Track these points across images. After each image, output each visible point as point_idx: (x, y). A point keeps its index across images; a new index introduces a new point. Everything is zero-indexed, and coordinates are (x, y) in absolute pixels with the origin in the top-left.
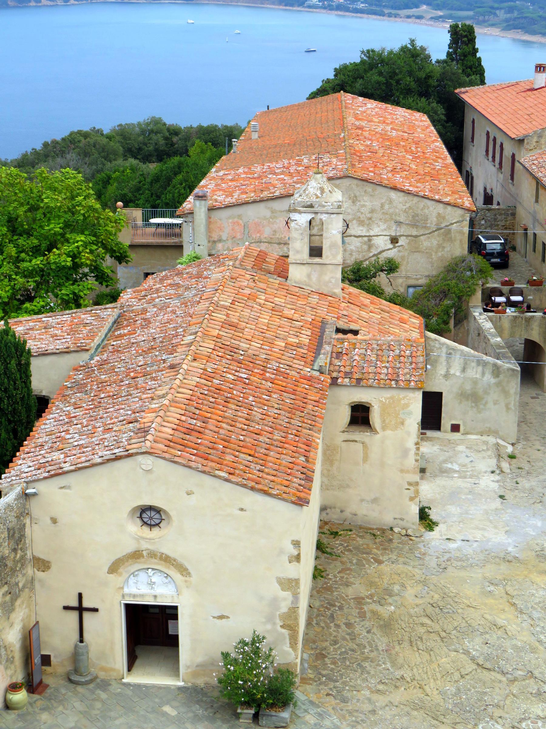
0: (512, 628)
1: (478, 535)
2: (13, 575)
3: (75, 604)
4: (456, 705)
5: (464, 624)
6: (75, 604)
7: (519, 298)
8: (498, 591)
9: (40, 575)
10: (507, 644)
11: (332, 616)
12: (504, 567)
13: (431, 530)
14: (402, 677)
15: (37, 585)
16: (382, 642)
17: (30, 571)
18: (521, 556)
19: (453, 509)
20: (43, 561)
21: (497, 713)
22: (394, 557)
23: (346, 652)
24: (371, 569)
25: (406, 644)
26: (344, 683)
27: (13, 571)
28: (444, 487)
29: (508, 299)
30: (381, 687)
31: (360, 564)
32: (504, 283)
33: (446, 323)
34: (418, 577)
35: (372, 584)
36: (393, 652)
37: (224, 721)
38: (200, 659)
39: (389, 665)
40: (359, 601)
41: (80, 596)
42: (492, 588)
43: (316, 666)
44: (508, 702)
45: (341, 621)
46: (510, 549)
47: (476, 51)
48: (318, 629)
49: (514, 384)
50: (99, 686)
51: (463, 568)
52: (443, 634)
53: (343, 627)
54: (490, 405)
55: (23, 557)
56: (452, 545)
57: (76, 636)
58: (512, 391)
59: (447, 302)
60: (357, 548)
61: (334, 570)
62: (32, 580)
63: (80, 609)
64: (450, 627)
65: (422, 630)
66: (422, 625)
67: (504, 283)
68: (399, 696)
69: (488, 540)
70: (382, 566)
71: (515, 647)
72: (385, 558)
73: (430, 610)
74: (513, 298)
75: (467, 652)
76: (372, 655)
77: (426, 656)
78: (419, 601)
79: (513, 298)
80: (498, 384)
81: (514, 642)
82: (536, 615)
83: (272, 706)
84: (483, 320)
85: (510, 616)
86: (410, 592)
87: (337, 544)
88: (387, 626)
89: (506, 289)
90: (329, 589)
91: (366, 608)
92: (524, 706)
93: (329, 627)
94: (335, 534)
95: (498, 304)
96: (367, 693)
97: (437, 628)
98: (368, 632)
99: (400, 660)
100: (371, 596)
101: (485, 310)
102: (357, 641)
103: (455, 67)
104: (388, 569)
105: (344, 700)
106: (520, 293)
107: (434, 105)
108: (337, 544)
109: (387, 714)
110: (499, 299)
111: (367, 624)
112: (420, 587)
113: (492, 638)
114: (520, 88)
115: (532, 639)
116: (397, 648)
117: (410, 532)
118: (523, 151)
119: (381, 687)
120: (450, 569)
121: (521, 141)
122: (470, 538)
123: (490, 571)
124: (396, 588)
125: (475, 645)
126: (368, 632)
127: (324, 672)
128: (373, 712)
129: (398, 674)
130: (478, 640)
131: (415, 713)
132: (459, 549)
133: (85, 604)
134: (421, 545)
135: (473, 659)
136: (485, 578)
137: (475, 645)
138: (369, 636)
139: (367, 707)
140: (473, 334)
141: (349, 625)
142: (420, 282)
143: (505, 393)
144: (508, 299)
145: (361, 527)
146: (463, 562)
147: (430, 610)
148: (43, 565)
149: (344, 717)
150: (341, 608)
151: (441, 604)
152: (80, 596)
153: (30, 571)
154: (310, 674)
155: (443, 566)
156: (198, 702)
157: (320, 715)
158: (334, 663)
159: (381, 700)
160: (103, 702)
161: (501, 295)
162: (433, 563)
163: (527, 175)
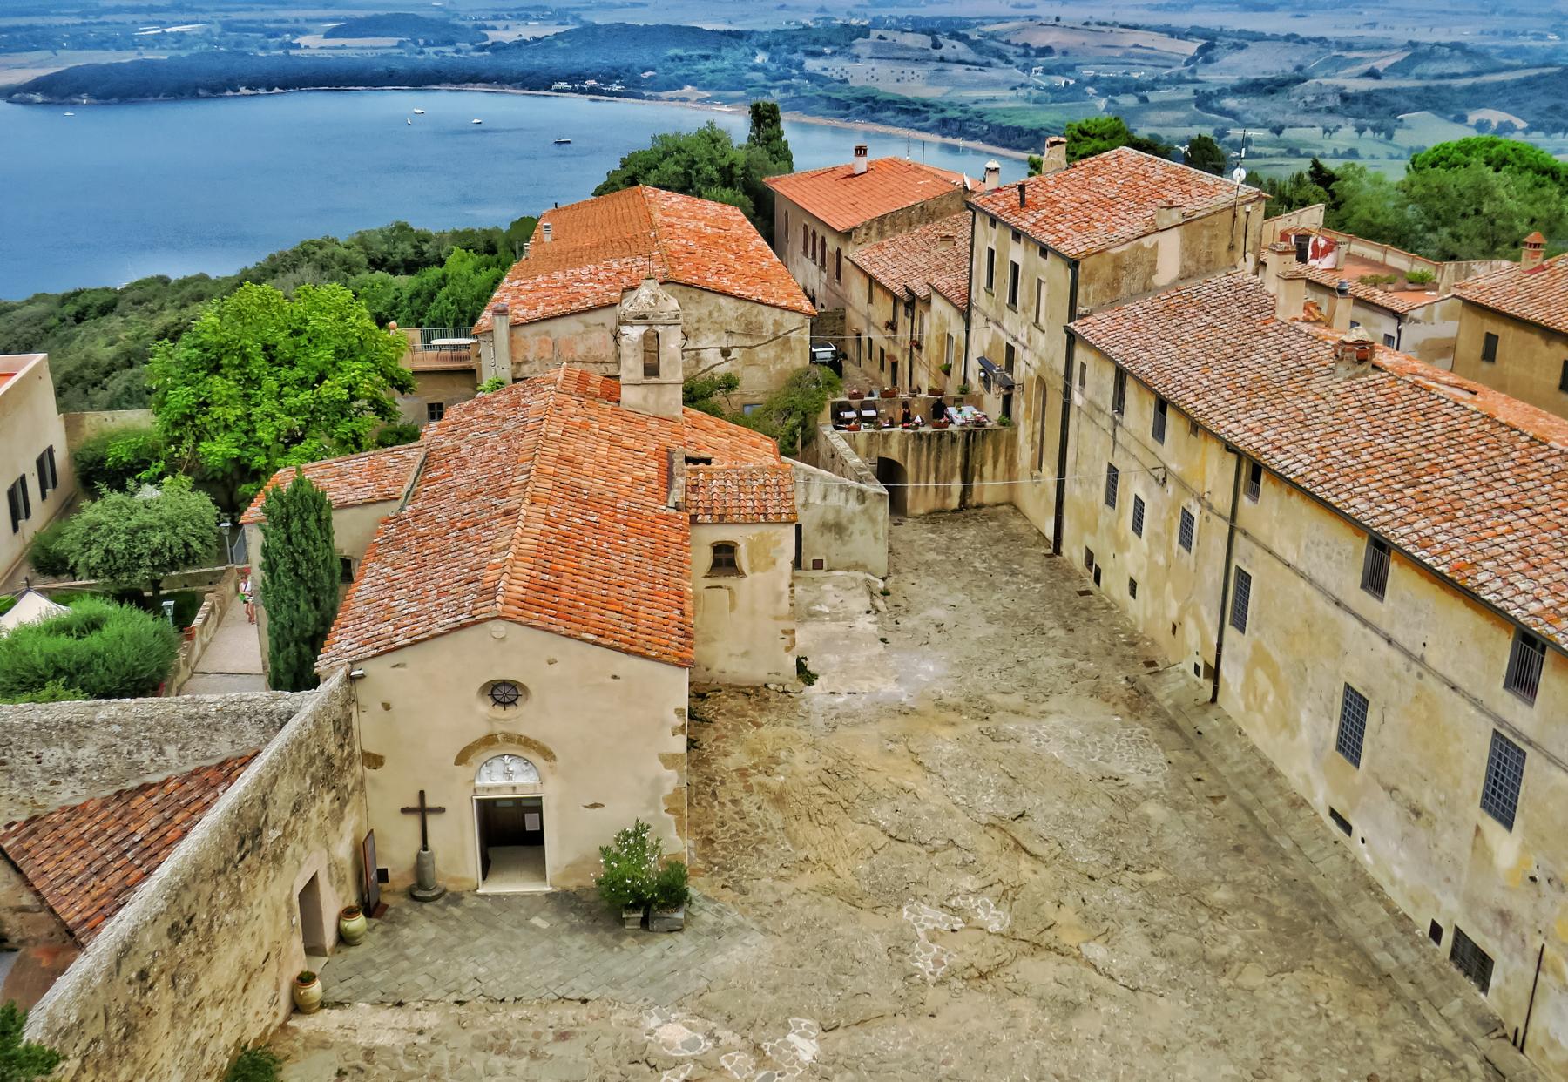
0: (923, 791)
1: (866, 686)
2: (340, 777)
3: (415, 803)
4: (873, 886)
5: (867, 791)
6: (415, 803)
7: (872, 413)
8: (899, 748)
9: (371, 773)
10: (919, 809)
11: (714, 793)
12: (901, 720)
13: (811, 683)
14: (807, 859)
15: (368, 786)
16: (776, 818)
17: (358, 769)
18: (918, 706)
19: (832, 658)
20: (375, 756)
21: (921, 891)
22: (773, 717)
23: (736, 835)
24: (750, 734)
25: (805, 819)
26: (740, 871)
27: (341, 771)
28: (817, 633)
29: (859, 414)
30: (783, 872)
31: (735, 729)
32: (853, 396)
33: (792, 444)
34: (805, 740)
35: (753, 752)
36: (791, 830)
37: (607, 929)
38: (570, 857)
39: (788, 846)
40: (743, 773)
41: (422, 794)
42: (892, 746)
43: (704, 855)
44: (931, 877)
45: (725, 798)
46: (904, 700)
47: (780, 134)
48: (698, 809)
49: (883, 511)
50: (449, 901)
51: (855, 725)
52: (845, 804)
53: (729, 805)
54: (856, 536)
55: (350, 754)
56: (839, 700)
57: (418, 843)
58: (881, 518)
59: (793, 421)
60: (730, 711)
61: (707, 737)
62: (362, 782)
63: (422, 810)
64: (851, 796)
65: (821, 801)
66: (820, 795)
67: (853, 396)
68: (807, 881)
69: (878, 691)
70: (762, 730)
71: (929, 813)
72: (764, 720)
73: (826, 777)
74: (865, 413)
75: (875, 823)
76: (769, 835)
77: (830, 831)
78: (812, 768)
79: (865, 413)
80: (865, 511)
81: (928, 807)
82: (947, 774)
83: (662, 907)
84: (835, 439)
85: (917, 777)
86: (799, 758)
87: (706, 708)
88: (779, 799)
89: (855, 402)
90: (706, 761)
91: (751, 780)
92: (950, 881)
93: (712, 807)
94: (703, 697)
95: (849, 421)
96: (769, 880)
97: (838, 798)
98: (759, 808)
99: (801, 839)
100: (755, 766)
101: (837, 428)
102: (748, 820)
103: (761, 153)
104: (769, 732)
105: (744, 892)
106: (873, 406)
107: (741, 196)
108: (706, 708)
109: (796, 903)
110: (852, 415)
111: (756, 798)
112: (810, 751)
113: (902, 804)
114: (837, 175)
115: (948, 802)
116: (795, 825)
117: (787, 688)
118: (850, 246)
119: (783, 872)
120: (840, 727)
121: (847, 235)
122: (856, 690)
123: (886, 726)
124: (783, 754)
125: (883, 814)
126: (759, 808)
127: (716, 860)
128: (779, 902)
129: (801, 855)
130: (887, 808)
131: (828, 899)
132: (846, 704)
133: (429, 803)
134: (802, 702)
135: (884, 831)
136: (882, 735)
137: (883, 814)
138: (761, 813)
139: (771, 897)
140: (824, 455)
141: (735, 802)
142: (757, 399)
143: (873, 521)
144: (859, 414)
145: (730, 686)
146: (852, 718)
147: (826, 777)
148: (374, 761)
149: (746, 911)
150: (722, 782)
151: (837, 769)
152: (422, 794)
153: (358, 769)
154: (700, 864)
155: (832, 724)
156: (573, 909)
157: (718, 912)
158: (725, 849)
159: (786, 888)
160: (458, 920)
161: (850, 409)
162: (820, 722)
163: (857, 273)
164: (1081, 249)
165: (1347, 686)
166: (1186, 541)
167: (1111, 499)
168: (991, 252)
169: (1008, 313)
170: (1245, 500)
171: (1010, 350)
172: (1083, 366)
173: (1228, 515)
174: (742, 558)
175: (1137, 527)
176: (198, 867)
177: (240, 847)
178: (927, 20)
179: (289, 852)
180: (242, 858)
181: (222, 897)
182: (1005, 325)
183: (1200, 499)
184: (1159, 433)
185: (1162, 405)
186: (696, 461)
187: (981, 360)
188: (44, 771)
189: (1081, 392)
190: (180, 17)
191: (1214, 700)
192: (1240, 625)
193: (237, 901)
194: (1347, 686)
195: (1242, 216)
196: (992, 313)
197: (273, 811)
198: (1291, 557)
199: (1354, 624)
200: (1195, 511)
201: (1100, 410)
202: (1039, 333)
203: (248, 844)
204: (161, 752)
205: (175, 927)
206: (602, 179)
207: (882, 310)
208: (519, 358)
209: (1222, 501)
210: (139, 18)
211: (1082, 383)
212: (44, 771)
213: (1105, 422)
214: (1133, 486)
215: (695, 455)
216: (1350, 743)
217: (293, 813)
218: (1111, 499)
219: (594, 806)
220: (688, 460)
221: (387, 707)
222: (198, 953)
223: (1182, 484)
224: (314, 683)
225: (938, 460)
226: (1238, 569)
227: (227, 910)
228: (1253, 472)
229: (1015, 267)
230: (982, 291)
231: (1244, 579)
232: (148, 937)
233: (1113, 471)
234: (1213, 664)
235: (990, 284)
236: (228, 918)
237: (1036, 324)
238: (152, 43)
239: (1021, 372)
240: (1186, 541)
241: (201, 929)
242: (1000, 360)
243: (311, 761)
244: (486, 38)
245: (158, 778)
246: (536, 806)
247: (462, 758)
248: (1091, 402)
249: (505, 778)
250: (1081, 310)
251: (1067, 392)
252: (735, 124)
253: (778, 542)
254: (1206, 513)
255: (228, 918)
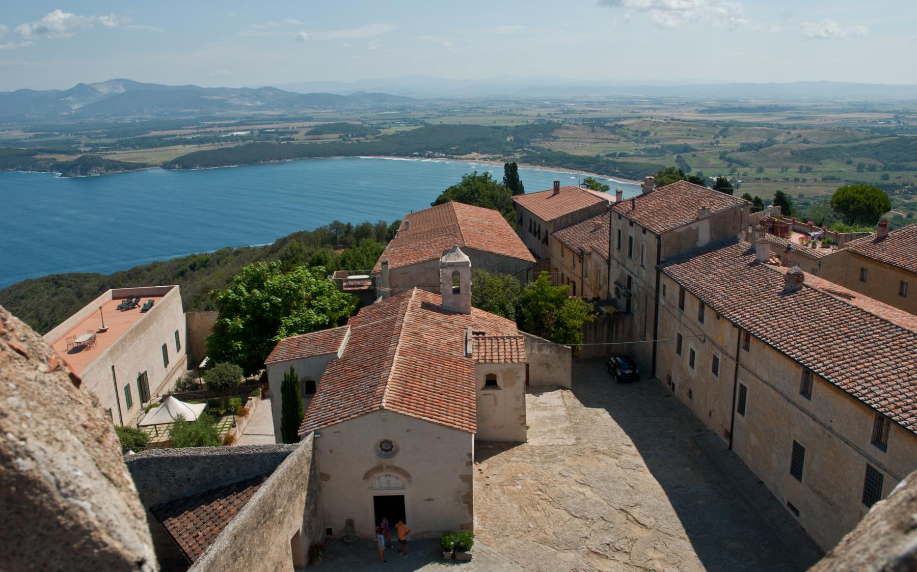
9: (324, 483)
73: (541, 487)
80: (559, 357)
92: (601, 537)
124: (520, 475)
135: (569, 513)
164: (662, 229)
165: (795, 442)
166: (715, 370)
167: (679, 351)
168: (619, 231)
169: (628, 260)
170: (742, 351)
171: (630, 278)
172: (664, 286)
173: (735, 356)
174: (500, 382)
175: (692, 364)
176: (245, 527)
177: (264, 517)
178: (589, 120)
179: (286, 520)
180: (265, 522)
181: (256, 541)
182: (627, 266)
183: (722, 350)
184: (701, 319)
185: (702, 305)
186: (477, 334)
187: (616, 283)
188: (176, 480)
189: (664, 299)
190: (240, 128)
191: (730, 448)
192: (742, 411)
193: (262, 542)
194: (795, 442)
195: (739, 214)
196: (620, 260)
197: (279, 500)
198: (766, 377)
199: (798, 411)
200: (719, 357)
201: (673, 307)
202: (643, 270)
203: (268, 515)
204: (228, 472)
205: (235, 553)
206: (434, 201)
207: (568, 259)
208: (394, 285)
209: (732, 351)
210: (222, 129)
211: (664, 294)
212: (176, 480)
213: (676, 312)
214: (689, 345)
215: (477, 331)
216: (797, 470)
217: (288, 501)
218: (679, 351)
219: (429, 500)
220: (474, 333)
221: (331, 451)
222: (245, 566)
223: (713, 342)
224: (298, 439)
225: (595, 331)
226: (741, 386)
227: (258, 546)
228: (746, 337)
229: (631, 238)
230: (615, 250)
231: (743, 389)
232: (222, 558)
233: (680, 338)
234: (729, 430)
235: (619, 247)
236: (258, 550)
237: (642, 265)
238: (225, 139)
239: (634, 288)
240: (715, 370)
241: (246, 555)
242: (625, 284)
243: (297, 477)
244: (380, 133)
245: (226, 484)
246: (400, 500)
247: (367, 476)
248: (669, 303)
249: (388, 485)
250: (662, 259)
251: (657, 299)
252: (497, 174)
253: (517, 373)
254: (725, 356)
255: (258, 550)
